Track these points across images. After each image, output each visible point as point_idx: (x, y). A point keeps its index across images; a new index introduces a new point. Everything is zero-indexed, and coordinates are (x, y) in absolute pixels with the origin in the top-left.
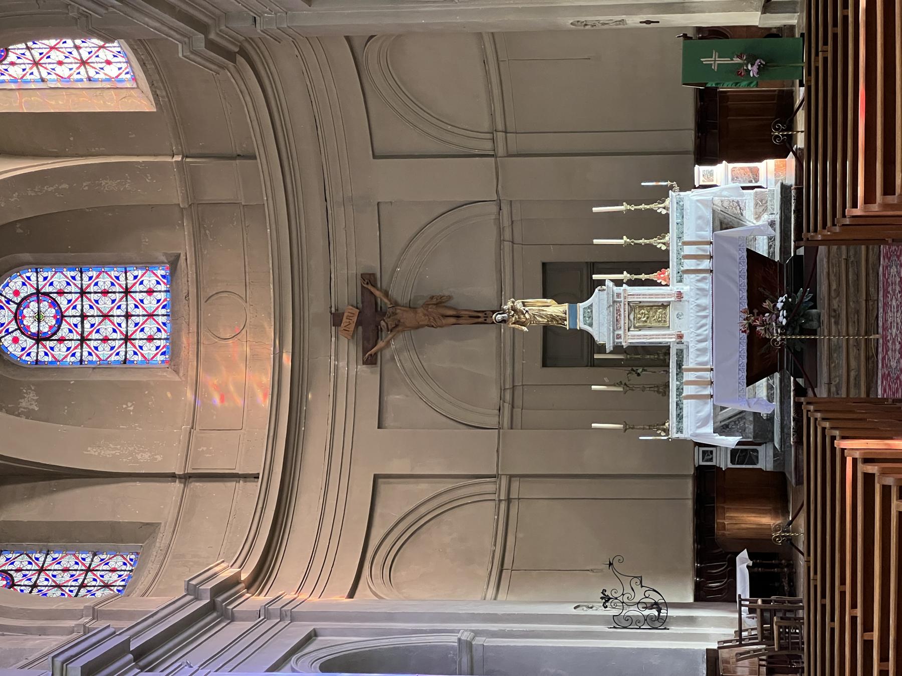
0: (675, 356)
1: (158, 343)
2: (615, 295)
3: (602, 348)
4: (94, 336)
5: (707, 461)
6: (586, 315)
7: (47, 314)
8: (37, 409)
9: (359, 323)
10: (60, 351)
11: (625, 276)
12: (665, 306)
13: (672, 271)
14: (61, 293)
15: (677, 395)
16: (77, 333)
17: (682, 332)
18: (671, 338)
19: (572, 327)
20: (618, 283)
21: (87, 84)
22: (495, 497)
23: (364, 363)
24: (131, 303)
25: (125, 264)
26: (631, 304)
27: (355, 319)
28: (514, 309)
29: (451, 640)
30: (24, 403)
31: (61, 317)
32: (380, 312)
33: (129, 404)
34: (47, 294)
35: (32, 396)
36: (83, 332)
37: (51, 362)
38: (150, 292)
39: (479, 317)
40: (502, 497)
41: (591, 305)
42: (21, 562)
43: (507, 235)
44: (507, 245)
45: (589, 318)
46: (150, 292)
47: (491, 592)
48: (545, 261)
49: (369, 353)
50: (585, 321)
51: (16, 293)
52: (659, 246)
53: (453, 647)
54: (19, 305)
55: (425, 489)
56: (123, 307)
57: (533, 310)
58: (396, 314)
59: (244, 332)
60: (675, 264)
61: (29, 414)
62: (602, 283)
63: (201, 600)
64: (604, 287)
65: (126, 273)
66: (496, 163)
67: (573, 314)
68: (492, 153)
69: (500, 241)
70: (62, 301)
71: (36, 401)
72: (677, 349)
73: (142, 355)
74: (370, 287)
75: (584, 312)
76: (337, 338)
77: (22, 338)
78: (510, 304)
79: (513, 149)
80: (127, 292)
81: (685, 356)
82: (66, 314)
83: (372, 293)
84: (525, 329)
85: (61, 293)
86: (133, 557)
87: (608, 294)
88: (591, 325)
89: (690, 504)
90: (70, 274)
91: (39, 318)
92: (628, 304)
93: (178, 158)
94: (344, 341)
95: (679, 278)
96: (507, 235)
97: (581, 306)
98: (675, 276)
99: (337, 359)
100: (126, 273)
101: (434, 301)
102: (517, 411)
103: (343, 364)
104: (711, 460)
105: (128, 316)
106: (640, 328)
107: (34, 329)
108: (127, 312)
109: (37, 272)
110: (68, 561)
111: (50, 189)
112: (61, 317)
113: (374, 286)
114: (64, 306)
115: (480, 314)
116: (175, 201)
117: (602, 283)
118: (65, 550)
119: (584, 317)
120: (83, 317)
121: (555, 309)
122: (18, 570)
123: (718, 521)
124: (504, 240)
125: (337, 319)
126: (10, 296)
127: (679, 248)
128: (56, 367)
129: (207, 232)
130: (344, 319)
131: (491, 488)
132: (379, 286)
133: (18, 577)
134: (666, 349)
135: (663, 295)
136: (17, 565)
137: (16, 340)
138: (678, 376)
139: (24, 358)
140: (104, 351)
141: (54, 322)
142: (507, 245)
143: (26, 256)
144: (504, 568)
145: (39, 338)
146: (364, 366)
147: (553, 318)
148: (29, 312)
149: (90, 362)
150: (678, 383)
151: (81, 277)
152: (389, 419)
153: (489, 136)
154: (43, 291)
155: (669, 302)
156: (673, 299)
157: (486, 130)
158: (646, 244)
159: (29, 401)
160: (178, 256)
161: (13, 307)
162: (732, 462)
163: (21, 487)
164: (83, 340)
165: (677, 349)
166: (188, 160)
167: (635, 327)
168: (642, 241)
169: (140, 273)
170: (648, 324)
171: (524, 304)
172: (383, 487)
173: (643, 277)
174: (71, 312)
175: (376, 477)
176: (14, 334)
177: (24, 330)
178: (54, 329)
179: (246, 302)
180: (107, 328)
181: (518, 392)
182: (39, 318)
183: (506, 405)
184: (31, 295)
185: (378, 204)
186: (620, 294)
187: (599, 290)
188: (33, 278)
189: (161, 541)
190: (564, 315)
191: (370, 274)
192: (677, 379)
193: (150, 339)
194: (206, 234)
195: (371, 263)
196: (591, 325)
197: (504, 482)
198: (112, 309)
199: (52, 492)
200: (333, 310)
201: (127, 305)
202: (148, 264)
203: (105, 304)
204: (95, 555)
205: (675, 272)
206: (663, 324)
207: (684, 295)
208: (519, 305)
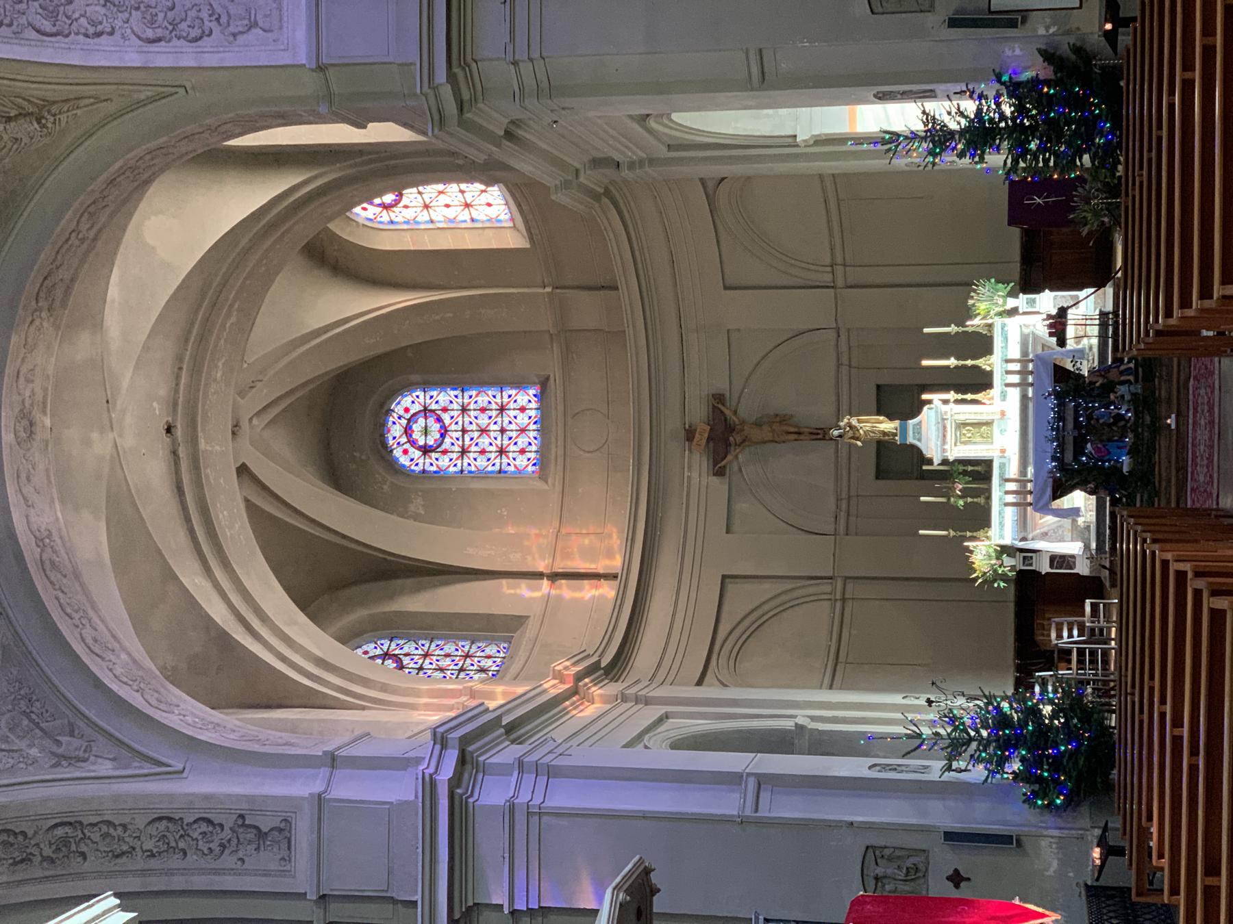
1: (529, 455)
3: (930, 462)
4: (473, 448)
5: (1027, 565)
7: (433, 429)
8: (423, 513)
9: (709, 439)
10: (444, 461)
11: (952, 396)
12: (988, 424)
13: (995, 392)
14: (445, 410)
16: (459, 446)
19: (903, 442)
20: (946, 402)
21: (469, 224)
22: (832, 597)
23: (714, 475)
24: (506, 420)
25: (501, 384)
27: (706, 435)
28: (851, 427)
29: (789, 724)
30: (412, 508)
31: (444, 432)
32: (730, 429)
33: (503, 510)
34: (433, 411)
35: (420, 501)
36: (463, 445)
37: (435, 472)
38: (523, 409)
39: (818, 434)
40: (838, 597)
41: (921, 422)
42: (409, 647)
43: (845, 360)
44: (844, 369)
46: (523, 409)
47: (827, 681)
48: (879, 383)
49: (719, 465)
50: (914, 436)
51: (407, 410)
52: (984, 367)
53: (790, 731)
54: (409, 420)
55: (768, 589)
56: (500, 423)
57: (867, 427)
59: (606, 446)
61: (416, 517)
62: (930, 402)
63: (564, 683)
65: (502, 392)
66: (835, 294)
67: (904, 430)
68: (832, 284)
69: (839, 365)
70: (446, 418)
71: (423, 506)
73: (515, 466)
74: (720, 406)
75: (914, 428)
76: (690, 450)
77: (411, 450)
79: (850, 281)
80: (502, 409)
82: (449, 429)
83: (722, 412)
84: (859, 443)
85: (445, 410)
86: (506, 645)
87: (936, 412)
88: (919, 440)
89: (1012, 606)
90: (453, 393)
91: (426, 432)
93: (549, 289)
94: (696, 456)
96: (845, 360)
97: (911, 422)
99: (690, 470)
100: (502, 392)
101: (778, 419)
102: (852, 519)
103: (695, 475)
104: (1031, 565)
105: (503, 431)
106: (965, 443)
107: (421, 443)
108: (502, 427)
109: (425, 392)
110: (450, 648)
111: (437, 317)
112: (444, 432)
113: (723, 405)
114: (447, 421)
115: (819, 431)
116: (545, 328)
117: (930, 402)
118: (447, 638)
120: (464, 431)
121: (887, 426)
122: (407, 655)
123: (1038, 621)
124: (842, 364)
125: (690, 434)
126: (402, 412)
128: (440, 475)
129: (574, 356)
130: (697, 435)
131: (827, 588)
132: (728, 404)
133: (406, 660)
134: (988, 463)
136: (406, 650)
137: (405, 452)
139: (413, 467)
140: (482, 462)
141: (438, 436)
142: (844, 369)
143: (415, 378)
144: (840, 660)
145: (426, 450)
146: (714, 477)
147: (884, 433)
148: (417, 427)
149: (470, 472)
151: (463, 396)
152: (736, 527)
153: (829, 269)
154: (429, 408)
157: (827, 264)
159: (417, 505)
160: (548, 378)
161: (404, 422)
162: (1051, 567)
163: (409, 582)
164: (464, 452)
166: (558, 291)
167: (961, 443)
168: (969, 362)
169: (513, 392)
171: (859, 421)
172: (731, 587)
173: (969, 396)
174: (453, 427)
175: (724, 577)
176: (405, 447)
177: (413, 443)
178: (439, 442)
179: (608, 418)
180: (484, 441)
181: (853, 502)
182: (426, 432)
183: (842, 514)
184: (420, 411)
185: (728, 331)
188: (422, 396)
189: (531, 630)
190: (895, 431)
191: (720, 395)
193: (522, 451)
194: (573, 358)
195: (722, 385)
196: (919, 440)
197: (839, 584)
198: (489, 424)
199: (435, 586)
200: (687, 426)
201: (502, 421)
202: (520, 385)
203: (483, 421)
204: (473, 643)
205: (999, 392)
206: (988, 439)
208: (854, 421)
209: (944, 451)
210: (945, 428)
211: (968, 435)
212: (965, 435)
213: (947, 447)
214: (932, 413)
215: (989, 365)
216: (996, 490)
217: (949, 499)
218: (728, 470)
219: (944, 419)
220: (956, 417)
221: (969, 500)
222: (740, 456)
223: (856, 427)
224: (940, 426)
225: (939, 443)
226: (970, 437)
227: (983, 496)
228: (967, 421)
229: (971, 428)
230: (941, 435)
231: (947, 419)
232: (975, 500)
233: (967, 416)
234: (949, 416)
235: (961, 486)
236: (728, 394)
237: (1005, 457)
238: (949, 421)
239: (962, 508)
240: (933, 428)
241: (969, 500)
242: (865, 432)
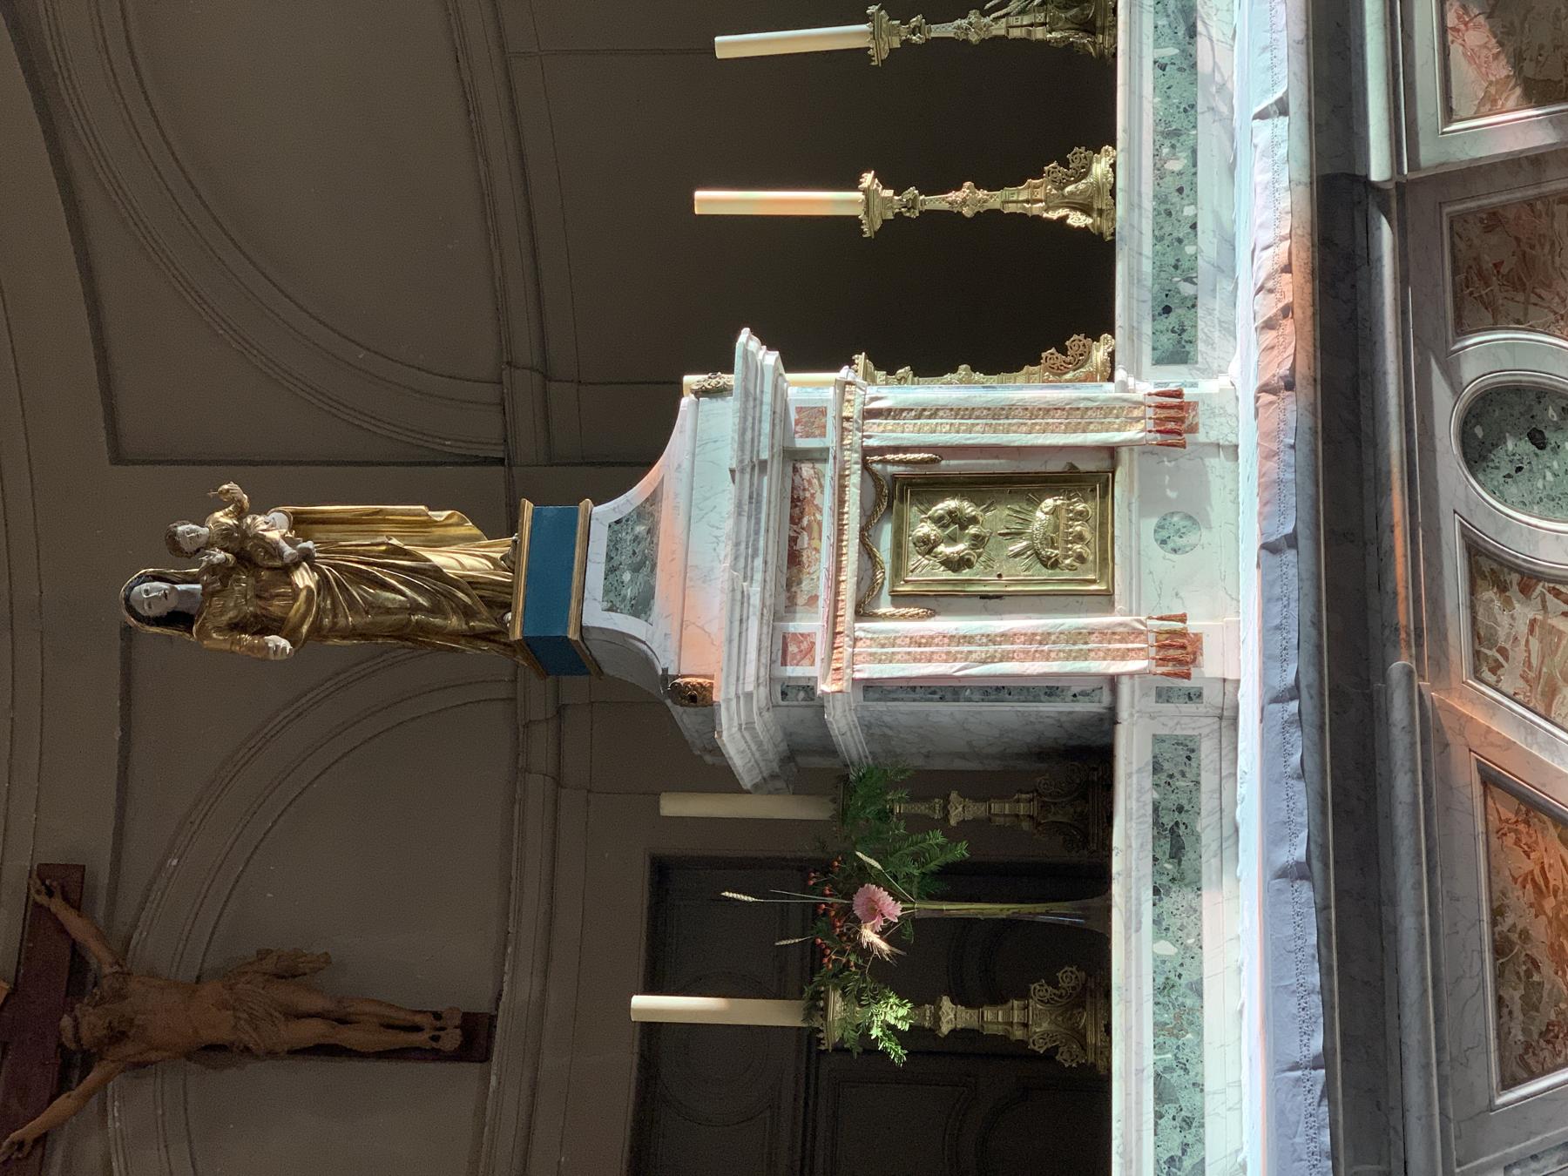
0: (1148, 782)
2: (793, 416)
6: (624, 558)
15: (1159, 1026)
17: (1193, 626)
18: (1124, 655)
26: (877, 467)
39: (417, 1029)
45: (636, 569)
50: (612, 588)
52: (1054, 215)
58: (125, 998)
60: (1147, 267)
64: (724, 379)
72: (1158, 739)
74: (57, 905)
75: (614, 545)
78: (223, 518)
81: (1208, 781)
83: (62, 930)
87: (750, 398)
88: (641, 606)
92: (865, 466)
95: (1167, 340)
97: (603, 514)
98: (1147, 328)
101: (269, 965)
106: (931, 601)
113: (76, 906)
115: (418, 1019)
119: (612, 570)
127: (1170, 183)
132: (100, 913)
135: (1075, 414)
138: (1167, 903)
150: (1167, 948)
155: (1112, 451)
156: (1133, 433)
158: (991, 217)
165: (1158, 739)
167: (898, 598)
168: (966, 198)
170: (979, 576)
171: (300, 523)
186: (823, 412)
187: (702, 393)
190: (502, 577)
192: (1157, 922)
205: (1147, 310)
207: (1202, 419)
208: (273, 527)
209: (783, 648)
210: (797, 504)
211: (961, 547)
212: (927, 546)
213: (810, 624)
214: (725, 414)
215: (1086, 209)
216: (1133, 925)
217: (817, 1006)
218: (57, 1158)
219: (794, 458)
220: (881, 434)
221: (951, 1016)
222: (114, 1110)
223: (272, 550)
224: (768, 485)
225: (755, 590)
226: (949, 563)
227: (1039, 989)
228: (950, 465)
229: (969, 509)
230: (769, 546)
231: (818, 456)
232: (993, 1018)
233: (945, 434)
234: (830, 440)
235: (893, 910)
236: (104, 878)
237: (1194, 696)
238: (829, 469)
239: (897, 1052)
240: (725, 497)
241: (951, 1016)
242: (324, 582)
